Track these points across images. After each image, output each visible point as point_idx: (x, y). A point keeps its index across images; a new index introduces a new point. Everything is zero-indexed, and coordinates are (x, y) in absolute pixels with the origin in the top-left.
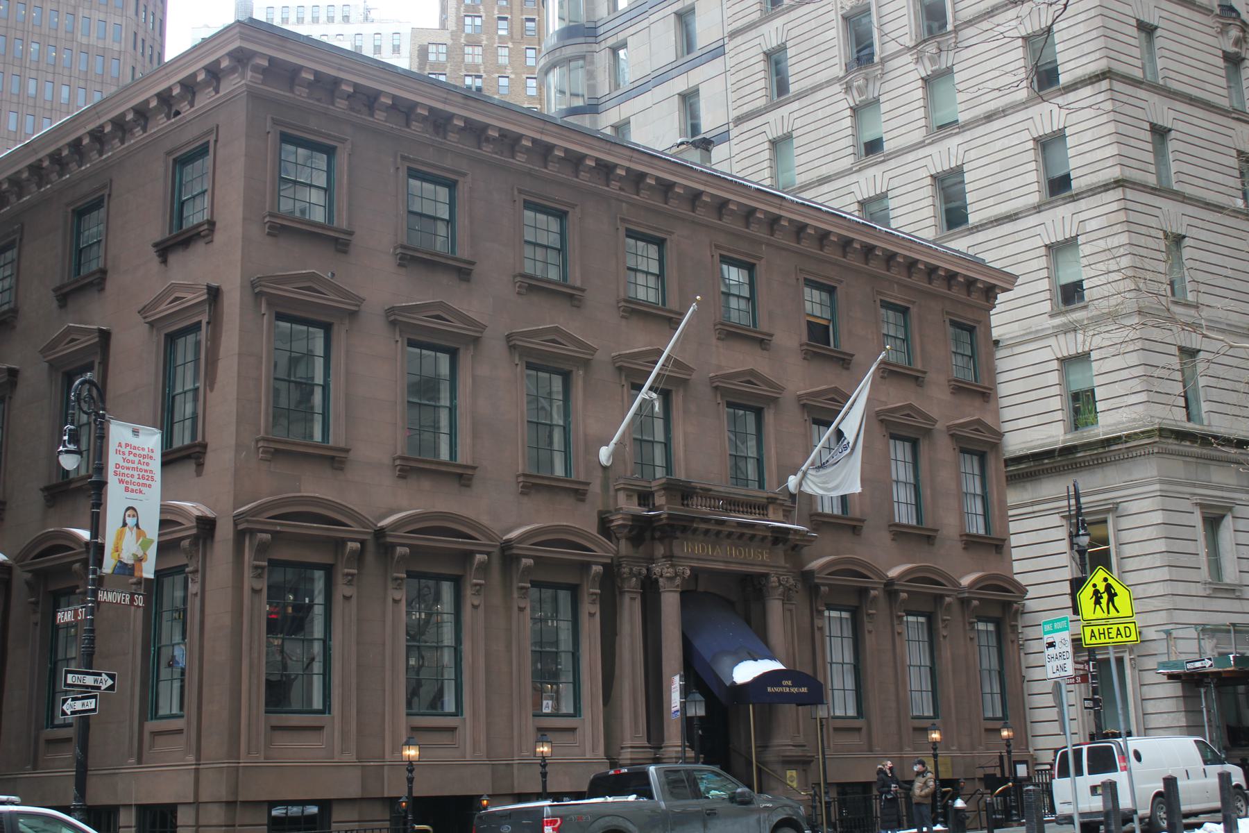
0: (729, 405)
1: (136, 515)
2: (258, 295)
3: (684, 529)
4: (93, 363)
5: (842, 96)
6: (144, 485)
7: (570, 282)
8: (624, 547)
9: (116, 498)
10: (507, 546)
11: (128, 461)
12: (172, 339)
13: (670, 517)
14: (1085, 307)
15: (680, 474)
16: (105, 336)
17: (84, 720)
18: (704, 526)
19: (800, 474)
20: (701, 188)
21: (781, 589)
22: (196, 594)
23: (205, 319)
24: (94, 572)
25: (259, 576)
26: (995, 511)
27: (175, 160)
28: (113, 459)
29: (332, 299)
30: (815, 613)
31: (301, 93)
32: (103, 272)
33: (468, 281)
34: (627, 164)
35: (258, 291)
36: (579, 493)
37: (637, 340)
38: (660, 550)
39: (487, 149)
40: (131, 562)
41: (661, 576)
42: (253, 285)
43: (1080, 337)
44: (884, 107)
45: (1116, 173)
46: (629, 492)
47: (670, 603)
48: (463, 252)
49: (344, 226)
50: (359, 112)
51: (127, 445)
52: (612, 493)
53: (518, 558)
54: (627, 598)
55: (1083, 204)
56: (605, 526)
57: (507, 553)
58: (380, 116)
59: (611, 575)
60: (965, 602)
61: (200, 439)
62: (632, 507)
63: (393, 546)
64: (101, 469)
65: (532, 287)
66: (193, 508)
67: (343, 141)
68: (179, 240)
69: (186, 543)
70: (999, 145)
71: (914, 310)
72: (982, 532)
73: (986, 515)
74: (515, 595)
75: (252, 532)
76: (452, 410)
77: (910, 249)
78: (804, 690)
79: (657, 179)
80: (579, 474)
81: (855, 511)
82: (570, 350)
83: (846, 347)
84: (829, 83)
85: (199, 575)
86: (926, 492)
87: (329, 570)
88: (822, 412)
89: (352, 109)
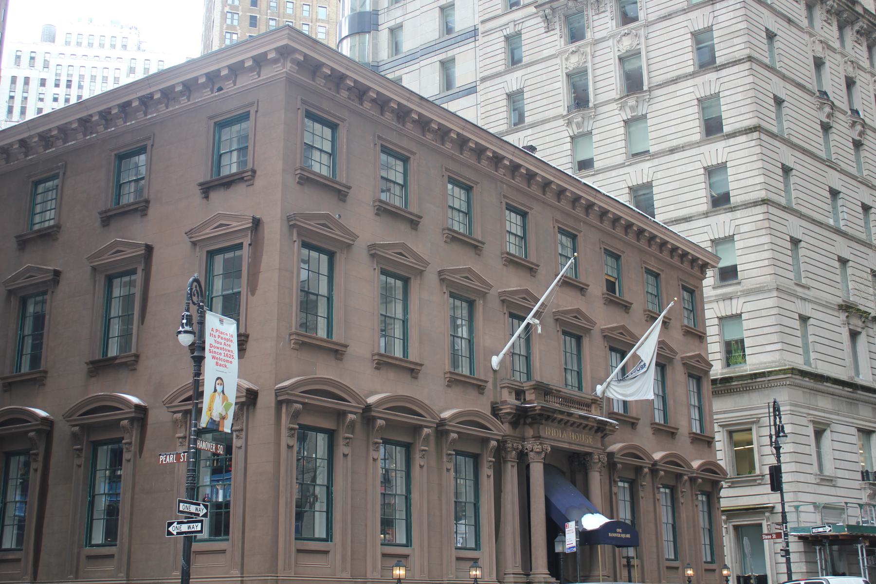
1: (222, 384)
2: (292, 227)
3: (548, 418)
4: (136, 269)
6: (228, 361)
7: (474, 236)
11: (218, 343)
12: (211, 254)
14: (739, 283)
15: (537, 377)
16: (149, 249)
18: (560, 417)
19: (605, 384)
20: (552, 179)
21: (599, 465)
22: (240, 448)
23: (246, 241)
24: (196, 426)
25: (292, 436)
26: (707, 417)
27: (215, 123)
28: (209, 341)
29: (337, 234)
31: (320, 81)
33: (416, 230)
34: (511, 157)
35: (293, 223)
36: (480, 388)
38: (530, 432)
39: (429, 136)
40: (217, 419)
41: (532, 451)
42: (289, 219)
43: (734, 301)
44: (595, 138)
45: (763, 194)
47: (537, 471)
50: (353, 100)
51: (217, 330)
52: (499, 389)
53: (447, 432)
54: (509, 465)
55: (738, 214)
57: (440, 428)
58: (367, 105)
60: (692, 480)
63: (375, 418)
65: (454, 238)
67: (343, 120)
70: (679, 170)
71: (663, 276)
72: (698, 432)
73: (701, 420)
74: (445, 459)
75: (289, 402)
77: (664, 234)
79: (527, 169)
80: (480, 374)
81: (633, 413)
83: (627, 298)
84: (555, 118)
85: (244, 433)
86: (670, 402)
89: (349, 98)
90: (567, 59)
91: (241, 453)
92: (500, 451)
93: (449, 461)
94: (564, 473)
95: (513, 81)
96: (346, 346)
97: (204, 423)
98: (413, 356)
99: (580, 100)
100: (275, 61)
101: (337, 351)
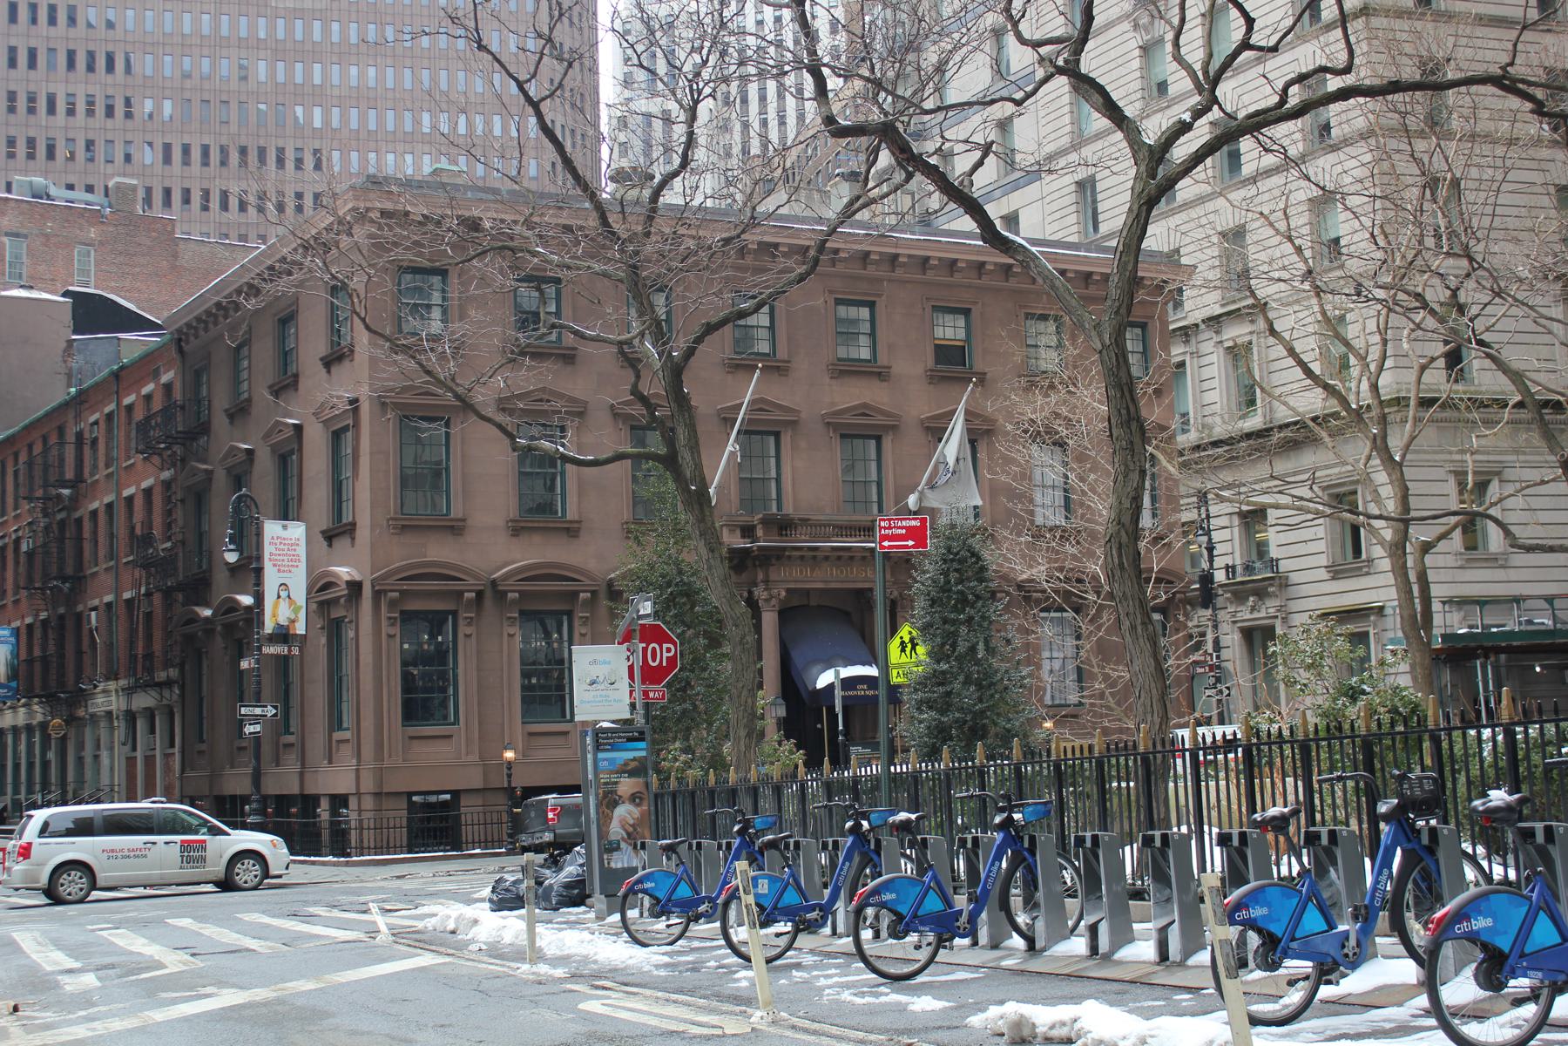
3: (779, 558)
9: (271, 579)
17: (257, 739)
23: (350, 422)
46: (732, 528)
47: (769, 620)
63: (505, 593)
66: (344, 572)
75: (385, 592)
94: (847, 614)
96: (464, 520)
97: (269, 627)
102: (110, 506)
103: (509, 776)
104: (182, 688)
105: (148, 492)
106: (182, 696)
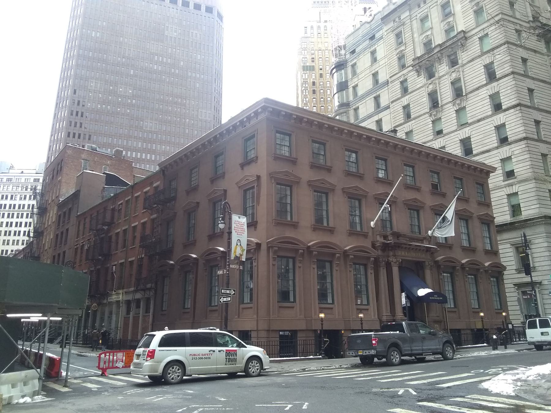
0: (409, 209)
1: (240, 242)
3: (399, 247)
5: (452, 107)
8: (380, 253)
10: (345, 251)
12: (245, 191)
13: (395, 243)
14: (516, 178)
15: (395, 230)
16: (225, 191)
17: (227, 303)
18: (405, 246)
19: (432, 230)
24: (229, 259)
25: (275, 260)
26: (494, 243)
28: (233, 225)
30: (439, 274)
32: (224, 173)
35: (271, 176)
36: (365, 236)
37: (381, 189)
38: (391, 253)
39: (334, 133)
42: (270, 174)
43: (514, 187)
44: (443, 120)
46: (381, 236)
47: (395, 270)
48: (329, 164)
49: (295, 157)
53: (348, 255)
54: (382, 269)
56: (373, 246)
58: (304, 124)
59: (376, 262)
60: (486, 271)
61: (255, 220)
62: (380, 239)
63: (312, 251)
64: (230, 228)
65: (348, 174)
68: (247, 163)
69: (252, 251)
70: (482, 129)
71: (464, 179)
72: (490, 249)
73: (491, 244)
74: (348, 266)
75: (272, 247)
76: (327, 211)
77: (463, 160)
78: (441, 298)
79: (385, 141)
81: (450, 242)
82: (361, 192)
83: (444, 190)
84: (424, 114)
86: (472, 236)
87: (294, 259)
88: (439, 211)
90: (428, 87)
91: (256, 268)
92: (376, 262)
93: (351, 267)
94: (413, 271)
95: (405, 101)
96: (298, 223)
97: (233, 257)
98: (331, 225)
99: (435, 104)
100: (261, 112)
101: (294, 225)
102: (125, 231)
103: (322, 324)
104: (156, 291)
105: (144, 224)
106: (156, 293)
